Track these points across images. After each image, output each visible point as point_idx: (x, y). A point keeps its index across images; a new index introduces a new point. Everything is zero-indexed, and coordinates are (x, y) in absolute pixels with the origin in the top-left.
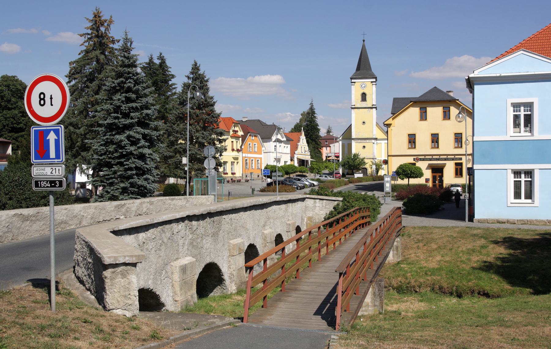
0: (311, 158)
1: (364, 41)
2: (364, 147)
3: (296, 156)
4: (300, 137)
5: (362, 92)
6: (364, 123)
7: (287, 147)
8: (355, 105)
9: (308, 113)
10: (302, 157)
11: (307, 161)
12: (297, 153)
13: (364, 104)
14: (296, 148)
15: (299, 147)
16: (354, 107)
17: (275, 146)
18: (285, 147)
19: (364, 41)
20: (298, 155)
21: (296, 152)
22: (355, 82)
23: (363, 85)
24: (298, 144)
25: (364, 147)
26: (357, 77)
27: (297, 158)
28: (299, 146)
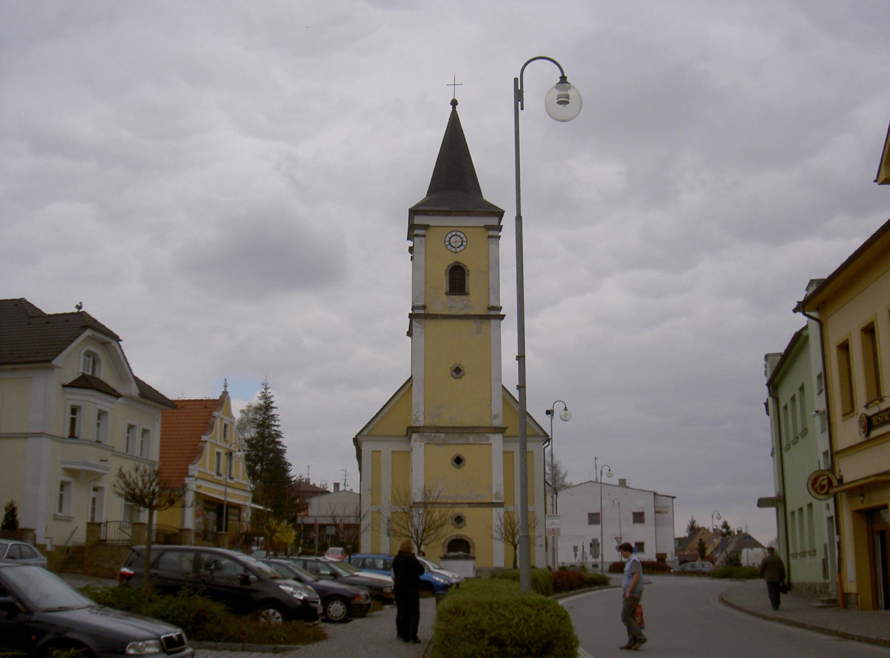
0: (254, 501)
1: (454, 103)
2: (458, 460)
3: (192, 485)
4: (215, 414)
5: (451, 260)
6: (457, 370)
7: (145, 432)
8: (424, 307)
9: (258, 409)
10: (215, 492)
11: (239, 508)
12: (196, 474)
13: (457, 304)
14: (196, 452)
15: (209, 452)
16: (422, 312)
17: (74, 410)
18: (131, 427)
19: (454, 103)
20: (199, 482)
21: (193, 469)
22: (426, 227)
23: (453, 240)
24: (204, 438)
25: (458, 460)
26: (436, 209)
27: (198, 495)
28: (208, 444)
